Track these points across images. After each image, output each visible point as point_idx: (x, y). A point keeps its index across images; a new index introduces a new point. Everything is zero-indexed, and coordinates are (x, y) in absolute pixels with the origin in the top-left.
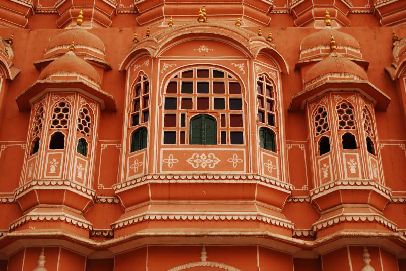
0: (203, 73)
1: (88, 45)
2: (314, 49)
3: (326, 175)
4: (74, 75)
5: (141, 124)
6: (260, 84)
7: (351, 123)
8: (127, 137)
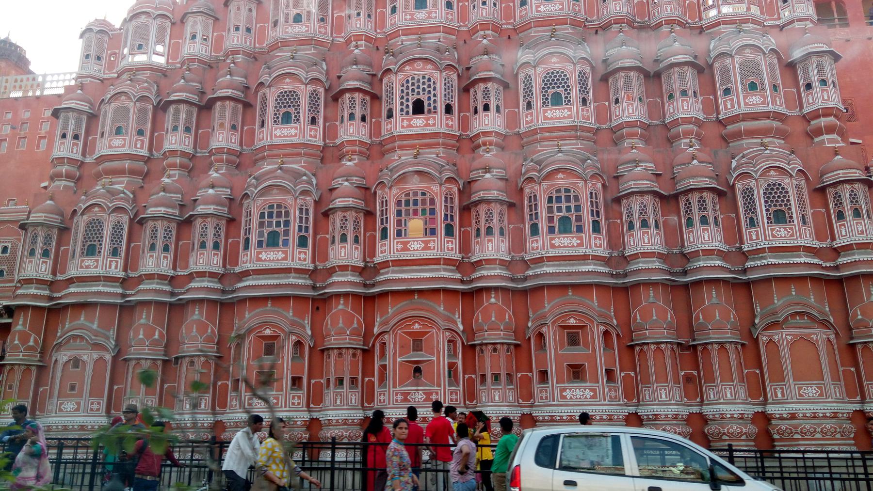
5: (385, 225)
6: (446, 198)
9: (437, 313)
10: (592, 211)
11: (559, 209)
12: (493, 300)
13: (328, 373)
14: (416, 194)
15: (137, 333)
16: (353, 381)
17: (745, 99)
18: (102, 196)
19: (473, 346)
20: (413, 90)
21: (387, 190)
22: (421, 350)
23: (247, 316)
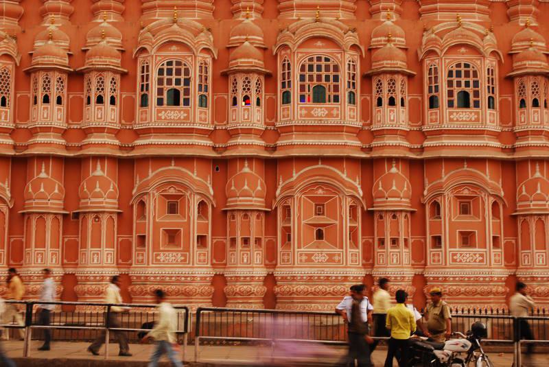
0: (319, 59)
1: (254, 35)
2: (379, 39)
3: (379, 119)
4: (250, 60)
5: (287, 89)
6: (349, 65)
7: (394, 91)
8: (279, 95)
9: (342, 181)
10: (489, 87)
11: (459, 84)
12: (394, 170)
13: (233, 231)
15: (36, 189)
16: (258, 241)
19: (373, 211)
21: (289, 51)
22: (323, 214)
23: (151, 174)
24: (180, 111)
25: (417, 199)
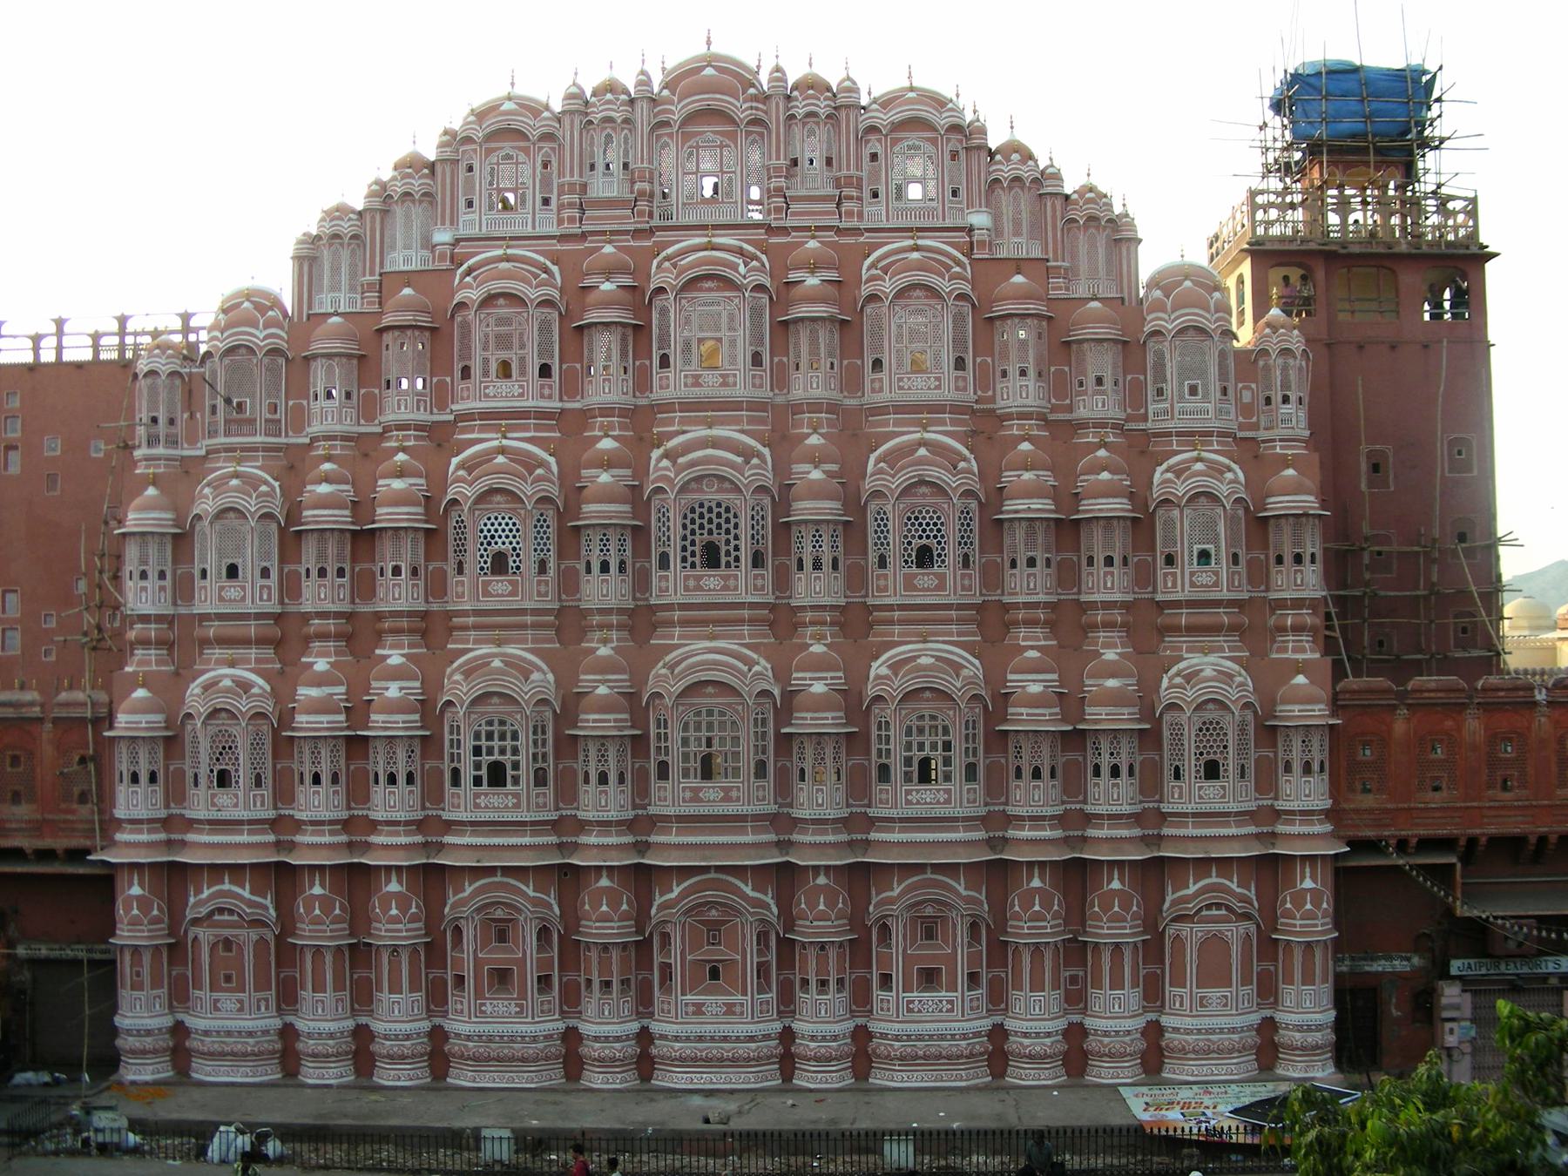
6: (756, 720)
12: (822, 880)
14: (710, 713)
17: (1192, 574)
18: (228, 690)
20: (702, 527)
22: (719, 944)
23: (469, 890)
24: (506, 795)
25: (857, 919)
